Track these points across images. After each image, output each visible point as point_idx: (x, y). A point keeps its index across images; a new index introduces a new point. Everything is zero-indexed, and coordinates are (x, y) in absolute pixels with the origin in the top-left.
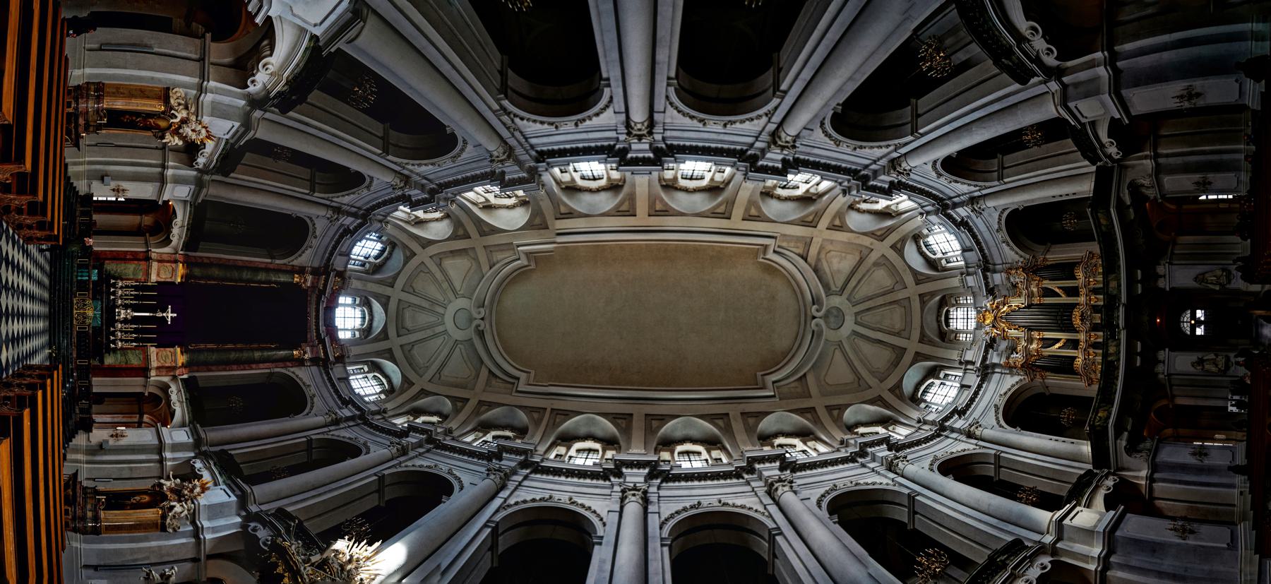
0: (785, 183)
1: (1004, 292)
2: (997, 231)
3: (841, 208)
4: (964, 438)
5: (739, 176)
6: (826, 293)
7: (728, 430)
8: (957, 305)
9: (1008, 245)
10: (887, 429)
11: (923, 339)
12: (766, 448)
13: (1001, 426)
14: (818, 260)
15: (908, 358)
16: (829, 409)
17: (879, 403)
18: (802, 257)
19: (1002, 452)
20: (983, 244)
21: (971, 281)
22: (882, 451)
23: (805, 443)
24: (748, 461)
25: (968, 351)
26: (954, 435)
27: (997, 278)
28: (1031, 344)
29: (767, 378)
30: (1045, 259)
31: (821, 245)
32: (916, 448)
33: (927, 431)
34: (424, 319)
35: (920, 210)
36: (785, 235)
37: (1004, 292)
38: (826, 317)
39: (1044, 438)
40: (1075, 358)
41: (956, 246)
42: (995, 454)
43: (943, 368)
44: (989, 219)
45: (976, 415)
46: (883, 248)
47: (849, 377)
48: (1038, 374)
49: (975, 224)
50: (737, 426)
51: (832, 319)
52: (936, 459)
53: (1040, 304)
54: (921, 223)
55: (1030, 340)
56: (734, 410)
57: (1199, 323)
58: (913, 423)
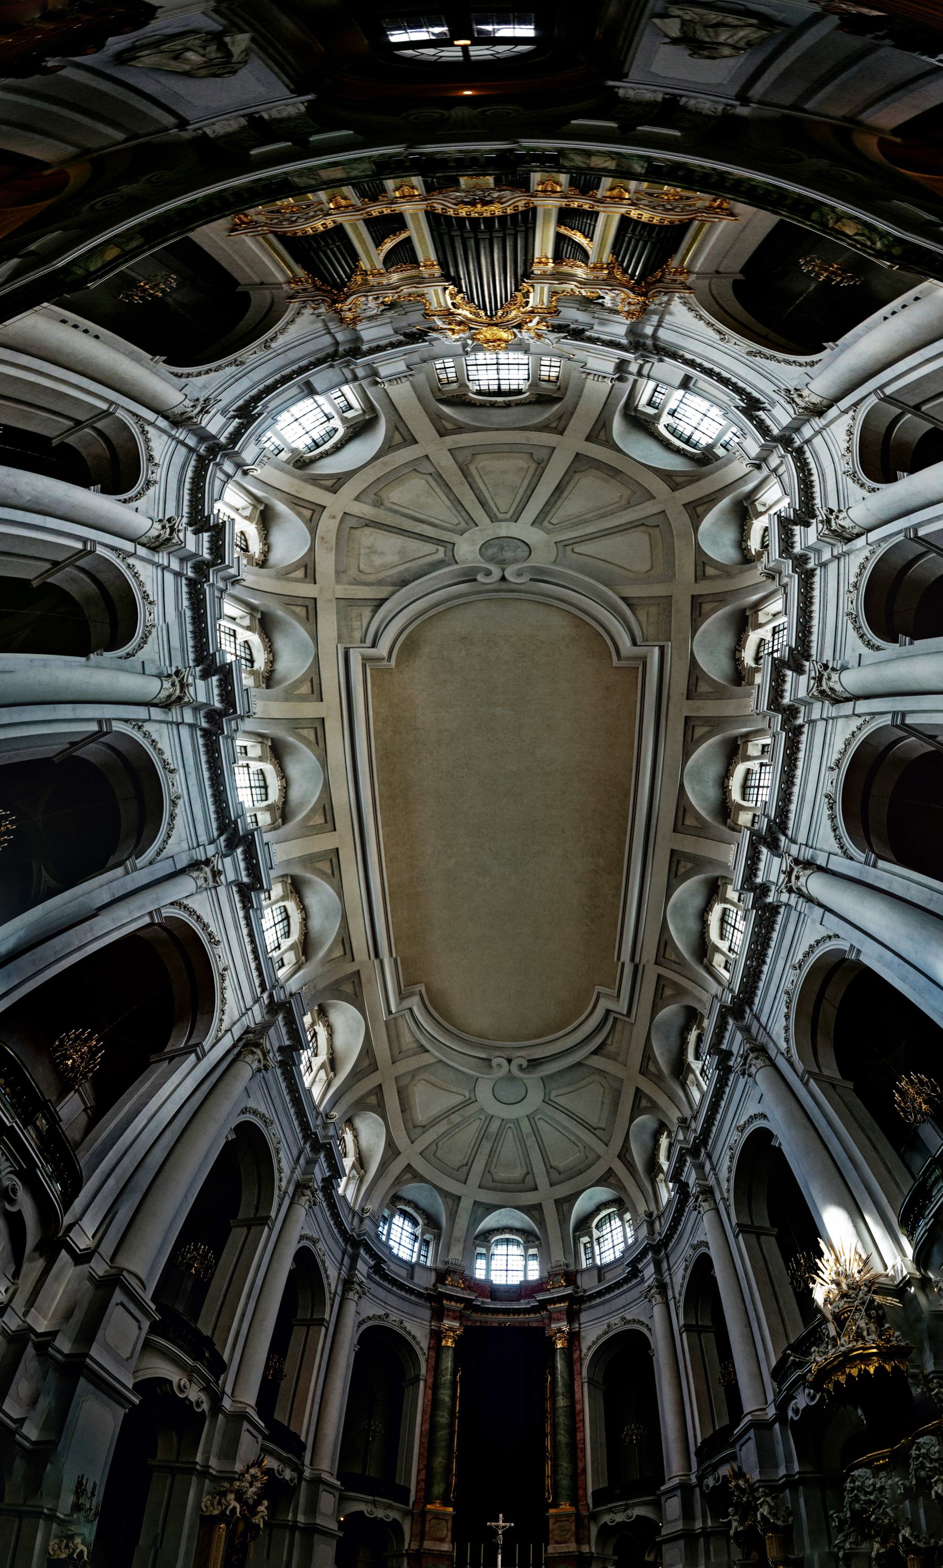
0: (243, 662)
3: (269, 576)
7: (715, 724)
12: (758, 679)
17: (700, 510)
18: (379, 606)
23: (761, 626)
24: (774, 710)
29: (623, 653)
34: (509, 1149)
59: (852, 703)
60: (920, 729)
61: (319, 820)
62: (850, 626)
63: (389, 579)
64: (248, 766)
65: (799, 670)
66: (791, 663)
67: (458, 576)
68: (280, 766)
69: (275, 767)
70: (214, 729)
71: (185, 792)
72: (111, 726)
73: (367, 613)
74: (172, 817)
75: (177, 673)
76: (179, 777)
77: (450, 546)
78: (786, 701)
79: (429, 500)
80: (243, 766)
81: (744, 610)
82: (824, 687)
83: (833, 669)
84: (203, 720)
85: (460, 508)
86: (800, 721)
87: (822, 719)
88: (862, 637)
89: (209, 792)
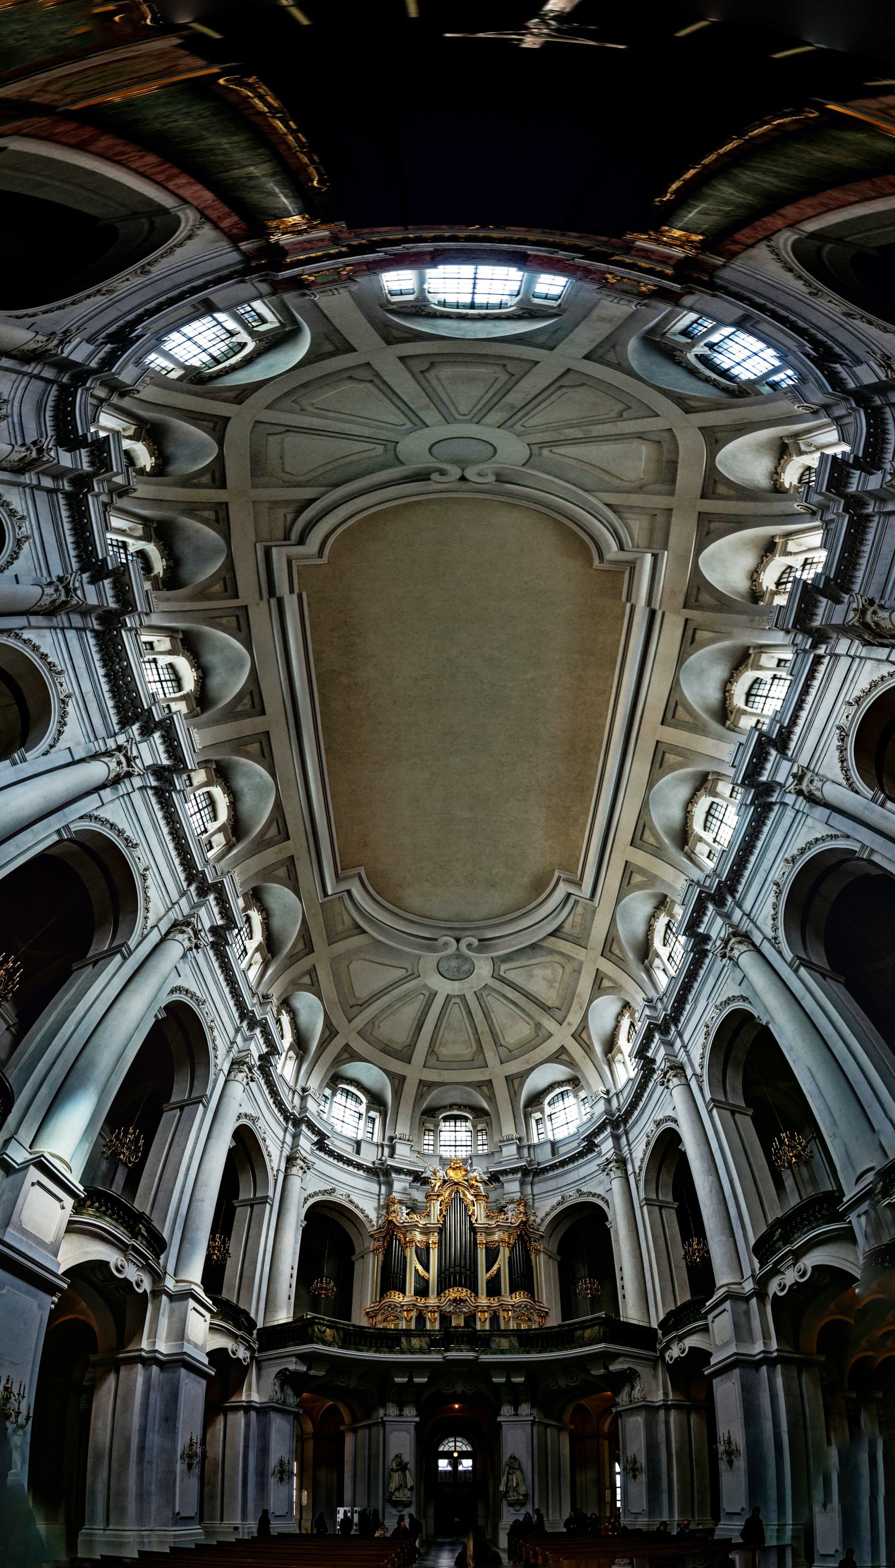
1: (493, 1196)
2: (579, 1191)
4: (287, 1152)
5: (697, 875)
6: (498, 957)
8: (475, 1132)
9: (559, 1204)
10: (289, 1049)
11: (425, 1086)
12: (241, 902)
13: (306, 1200)
14: (551, 952)
15: (397, 1067)
16: (312, 972)
19: (272, 1206)
20: (561, 1170)
21: (510, 1151)
22: (257, 1048)
23: (257, 950)
24: (216, 884)
25: (409, 1148)
26: (289, 1139)
27: (512, 1187)
28: (421, 1233)
29: (356, 881)
30: (538, 1251)
31: (574, 958)
32: (267, 1092)
33: (292, 1102)
35: (613, 1091)
36: (594, 912)
37: (493, 1196)
38: (459, 956)
39: (293, 1260)
40: (403, 1291)
41: (560, 1134)
42: (267, 1197)
43: (384, 1115)
44: (595, 1181)
45: (320, 1165)
46: (562, 1036)
47: (362, 992)
48: (381, 1243)
49: (589, 1162)
50: (270, 856)
51: (454, 963)
52: (254, 1120)
53: (476, 1244)
54: (595, 1090)
55: (426, 1231)
56: (297, 844)
57: (455, 1463)
58: (301, 1083)
59: (163, 933)
60: (107, 960)
61: (670, 758)
62: (198, 994)
63: (544, 953)
64: (715, 841)
65: (214, 930)
66: (222, 931)
67: (492, 945)
68: (686, 823)
69: (691, 825)
70: (724, 890)
71: (779, 860)
72: (792, 960)
73: (567, 927)
74: (802, 851)
75: (724, 956)
76: (775, 875)
77: (496, 975)
78: (211, 898)
79: (504, 1021)
80: (719, 843)
81: (273, 957)
82: (189, 930)
83: (190, 949)
84: (728, 904)
85: (485, 1010)
86: (193, 888)
87: (177, 903)
88: (187, 991)
89: (759, 844)
